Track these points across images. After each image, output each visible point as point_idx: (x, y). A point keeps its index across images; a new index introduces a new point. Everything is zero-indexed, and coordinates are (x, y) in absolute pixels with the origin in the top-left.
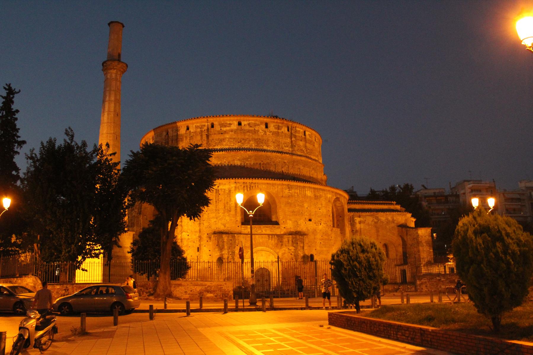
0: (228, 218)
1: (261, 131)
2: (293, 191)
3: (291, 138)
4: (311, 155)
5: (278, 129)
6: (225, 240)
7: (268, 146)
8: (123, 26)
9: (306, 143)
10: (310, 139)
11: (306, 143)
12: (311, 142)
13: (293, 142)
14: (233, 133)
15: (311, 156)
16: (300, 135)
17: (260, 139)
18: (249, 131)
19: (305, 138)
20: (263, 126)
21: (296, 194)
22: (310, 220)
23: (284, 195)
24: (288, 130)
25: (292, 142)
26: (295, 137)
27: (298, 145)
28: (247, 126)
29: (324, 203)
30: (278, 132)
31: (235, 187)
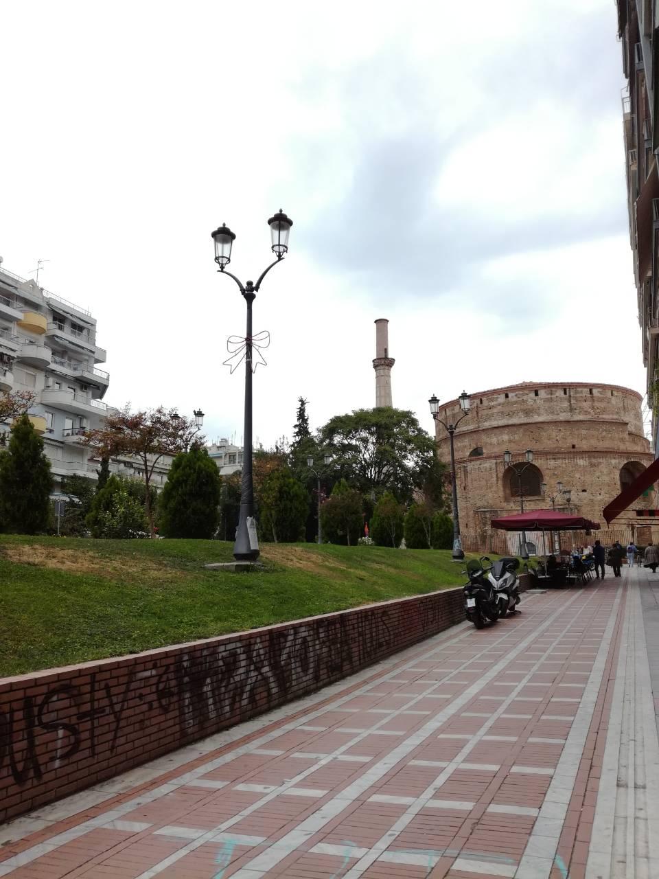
0: (490, 495)
1: (530, 400)
2: (559, 461)
3: (570, 401)
4: (602, 414)
5: (551, 394)
6: (488, 516)
7: (539, 415)
8: (388, 321)
9: (593, 401)
10: (602, 396)
11: (593, 401)
12: (601, 400)
13: (573, 405)
14: (499, 407)
15: (604, 416)
16: (584, 395)
17: (529, 409)
18: (516, 402)
19: (592, 397)
20: (533, 395)
21: (564, 465)
22: (584, 491)
23: (549, 467)
24: (565, 393)
25: (571, 405)
26: (576, 399)
27: (580, 407)
28: (515, 397)
29: (605, 471)
30: (551, 398)
31: (496, 463)
